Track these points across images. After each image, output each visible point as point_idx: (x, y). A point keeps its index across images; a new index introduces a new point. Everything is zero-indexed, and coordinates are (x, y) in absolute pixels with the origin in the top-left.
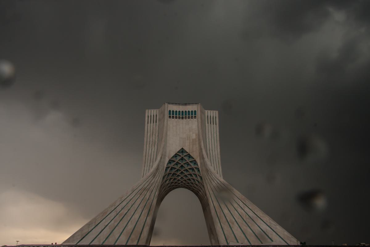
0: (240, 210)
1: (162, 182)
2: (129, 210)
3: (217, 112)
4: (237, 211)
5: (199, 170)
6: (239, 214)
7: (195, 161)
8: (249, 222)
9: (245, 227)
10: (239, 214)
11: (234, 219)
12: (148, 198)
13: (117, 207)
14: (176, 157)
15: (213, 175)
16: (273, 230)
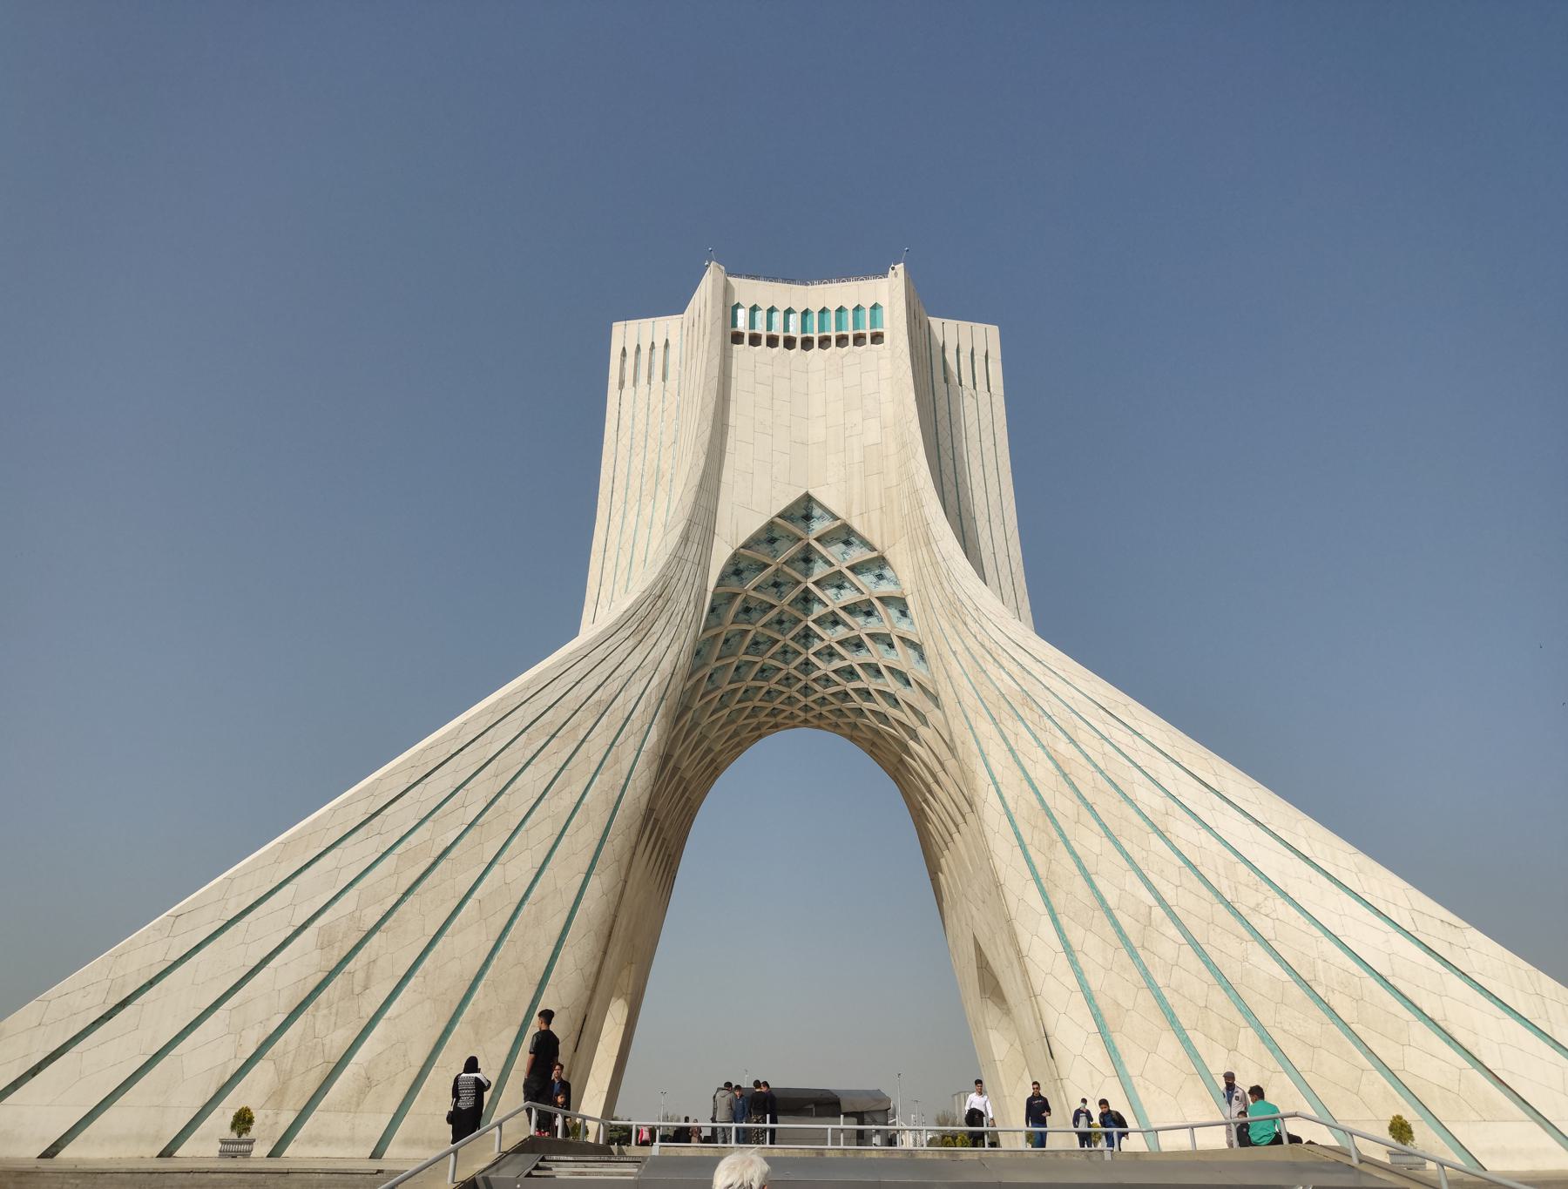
0: (1182, 830)
1: (690, 676)
2: (470, 826)
3: (994, 331)
4: (1162, 835)
5: (904, 614)
6: (1180, 854)
7: (881, 561)
8: (1256, 909)
9: (1230, 947)
10: (1180, 854)
11: (1151, 888)
12: (598, 758)
13: (385, 807)
14: (772, 541)
15: (990, 627)
16: (1445, 962)
